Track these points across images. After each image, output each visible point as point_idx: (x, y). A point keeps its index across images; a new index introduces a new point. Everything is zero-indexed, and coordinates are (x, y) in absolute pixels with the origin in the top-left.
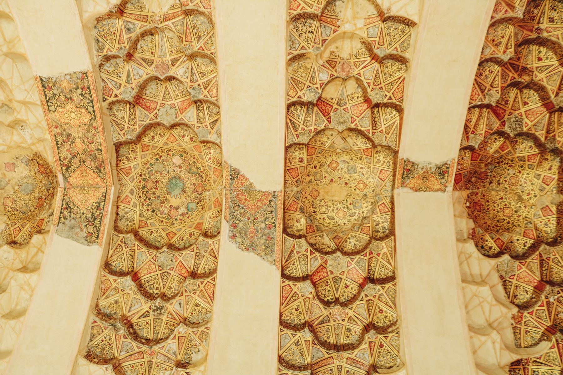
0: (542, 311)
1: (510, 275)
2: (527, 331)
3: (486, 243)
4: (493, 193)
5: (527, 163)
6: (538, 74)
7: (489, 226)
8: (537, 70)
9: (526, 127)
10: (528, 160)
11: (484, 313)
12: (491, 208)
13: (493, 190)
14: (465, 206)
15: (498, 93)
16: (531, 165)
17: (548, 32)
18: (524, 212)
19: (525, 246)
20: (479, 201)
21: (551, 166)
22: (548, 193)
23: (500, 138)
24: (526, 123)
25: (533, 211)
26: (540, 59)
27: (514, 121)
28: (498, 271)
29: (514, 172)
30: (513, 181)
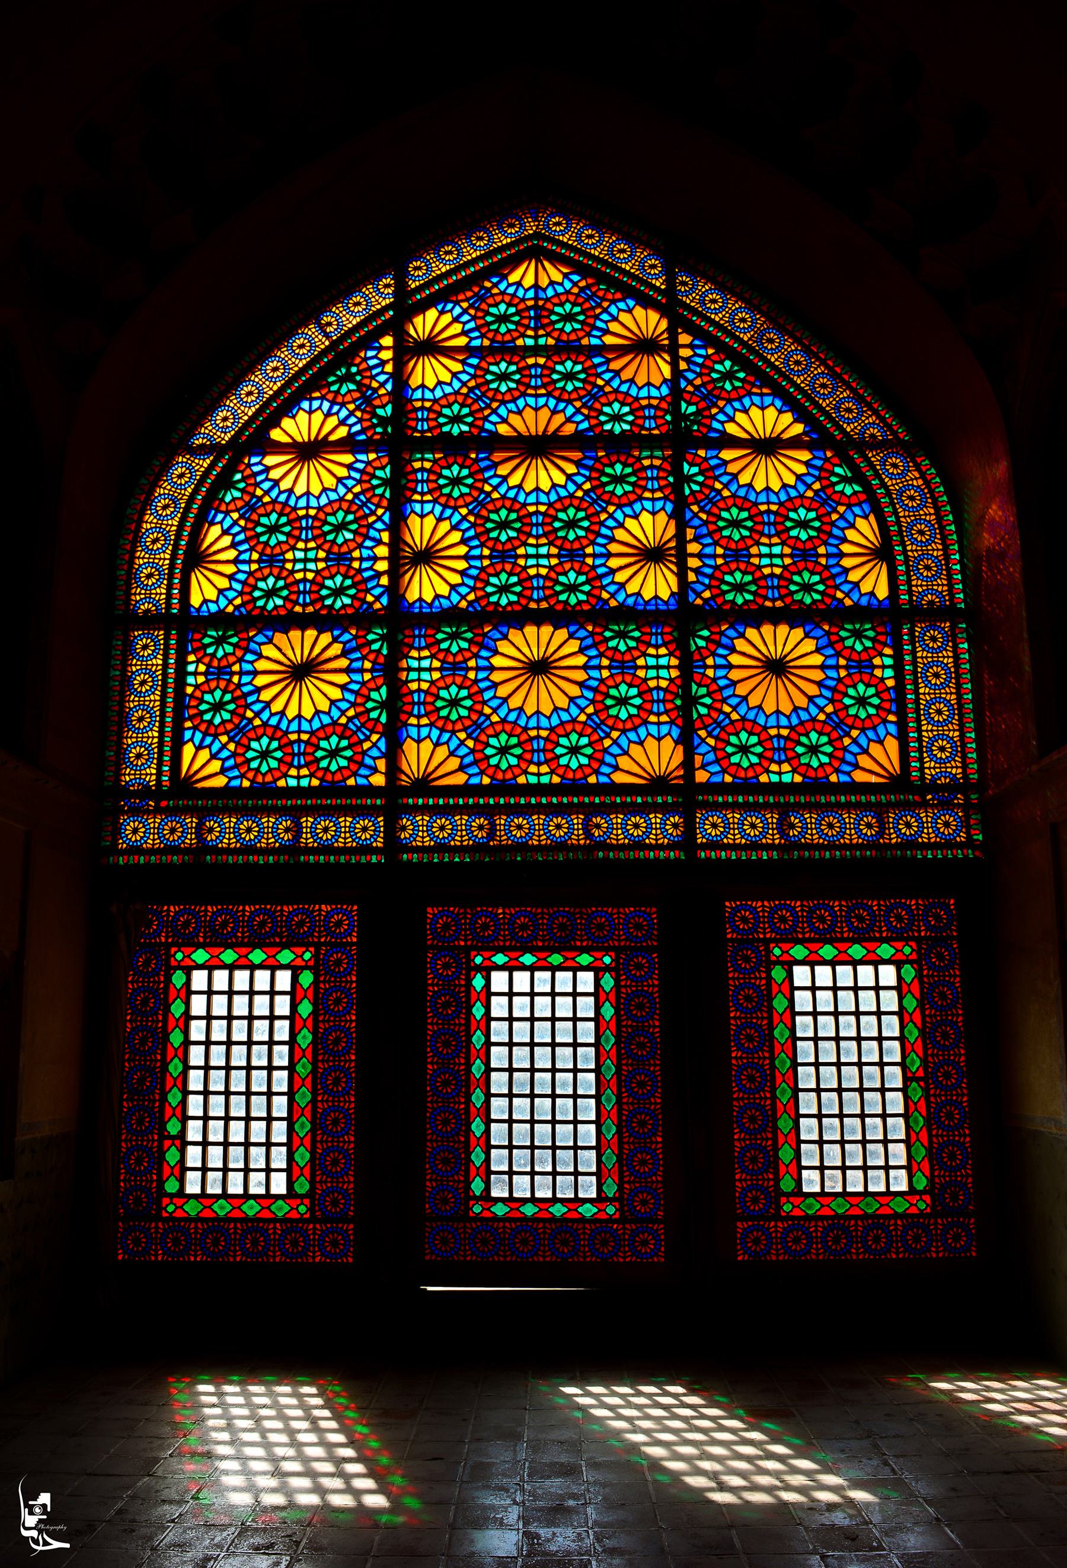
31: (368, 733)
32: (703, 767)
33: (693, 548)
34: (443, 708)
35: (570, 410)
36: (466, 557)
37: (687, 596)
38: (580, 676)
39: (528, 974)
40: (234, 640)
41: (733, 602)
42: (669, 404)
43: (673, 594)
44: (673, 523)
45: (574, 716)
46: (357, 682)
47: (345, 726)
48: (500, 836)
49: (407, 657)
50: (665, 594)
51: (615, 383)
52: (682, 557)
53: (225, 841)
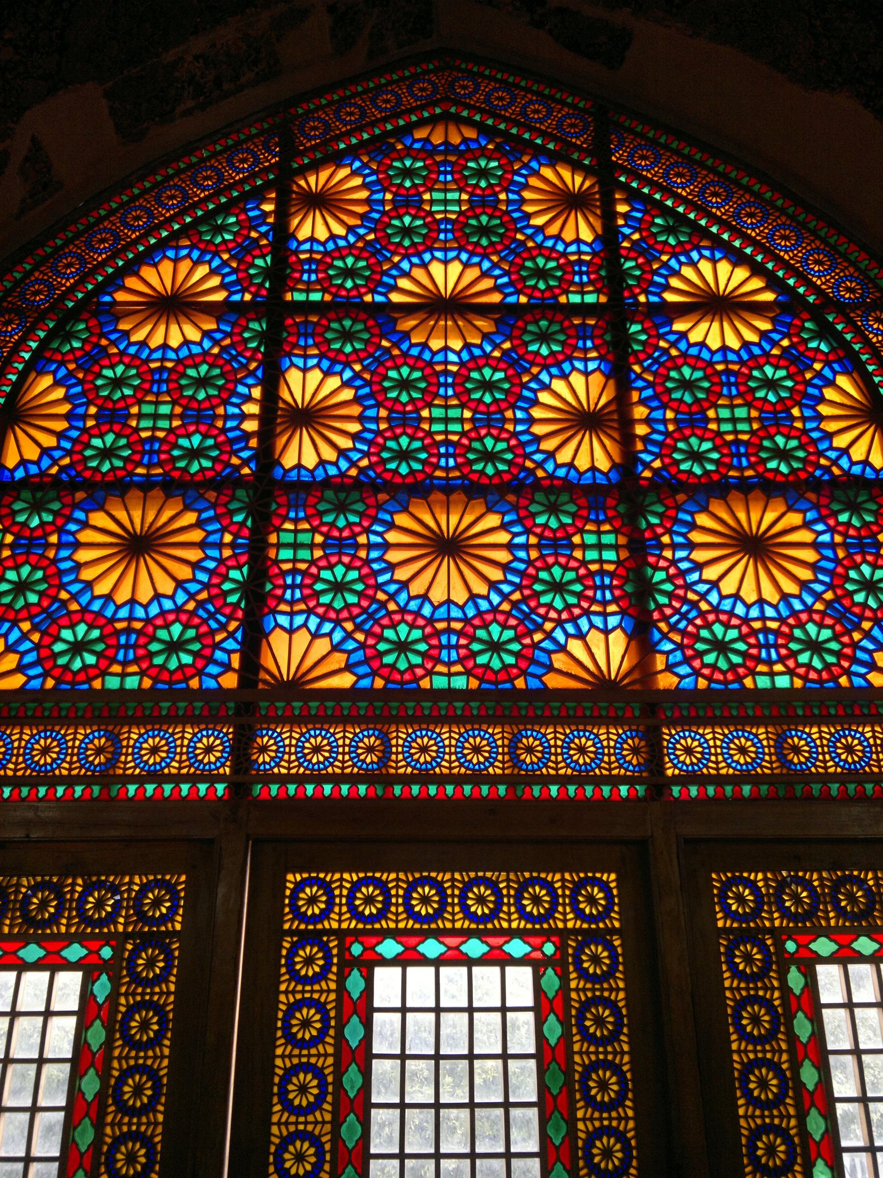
31: (223, 619)
32: (670, 668)
33: (640, 412)
34: (324, 592)
35: (486, 265)
36: (361, 419)
37: (636, 467)
38: (502, 556)
39: (432, 970)
40: (56, 506)
41: (690, 472)
42: (602, 259)
44: (611, 383)
46: (213, 559)
47: (193, 613)
48: (397, 762)
49: (279, 530)
50: (603, 464)
52: (627, 423)
53: (11, 766)
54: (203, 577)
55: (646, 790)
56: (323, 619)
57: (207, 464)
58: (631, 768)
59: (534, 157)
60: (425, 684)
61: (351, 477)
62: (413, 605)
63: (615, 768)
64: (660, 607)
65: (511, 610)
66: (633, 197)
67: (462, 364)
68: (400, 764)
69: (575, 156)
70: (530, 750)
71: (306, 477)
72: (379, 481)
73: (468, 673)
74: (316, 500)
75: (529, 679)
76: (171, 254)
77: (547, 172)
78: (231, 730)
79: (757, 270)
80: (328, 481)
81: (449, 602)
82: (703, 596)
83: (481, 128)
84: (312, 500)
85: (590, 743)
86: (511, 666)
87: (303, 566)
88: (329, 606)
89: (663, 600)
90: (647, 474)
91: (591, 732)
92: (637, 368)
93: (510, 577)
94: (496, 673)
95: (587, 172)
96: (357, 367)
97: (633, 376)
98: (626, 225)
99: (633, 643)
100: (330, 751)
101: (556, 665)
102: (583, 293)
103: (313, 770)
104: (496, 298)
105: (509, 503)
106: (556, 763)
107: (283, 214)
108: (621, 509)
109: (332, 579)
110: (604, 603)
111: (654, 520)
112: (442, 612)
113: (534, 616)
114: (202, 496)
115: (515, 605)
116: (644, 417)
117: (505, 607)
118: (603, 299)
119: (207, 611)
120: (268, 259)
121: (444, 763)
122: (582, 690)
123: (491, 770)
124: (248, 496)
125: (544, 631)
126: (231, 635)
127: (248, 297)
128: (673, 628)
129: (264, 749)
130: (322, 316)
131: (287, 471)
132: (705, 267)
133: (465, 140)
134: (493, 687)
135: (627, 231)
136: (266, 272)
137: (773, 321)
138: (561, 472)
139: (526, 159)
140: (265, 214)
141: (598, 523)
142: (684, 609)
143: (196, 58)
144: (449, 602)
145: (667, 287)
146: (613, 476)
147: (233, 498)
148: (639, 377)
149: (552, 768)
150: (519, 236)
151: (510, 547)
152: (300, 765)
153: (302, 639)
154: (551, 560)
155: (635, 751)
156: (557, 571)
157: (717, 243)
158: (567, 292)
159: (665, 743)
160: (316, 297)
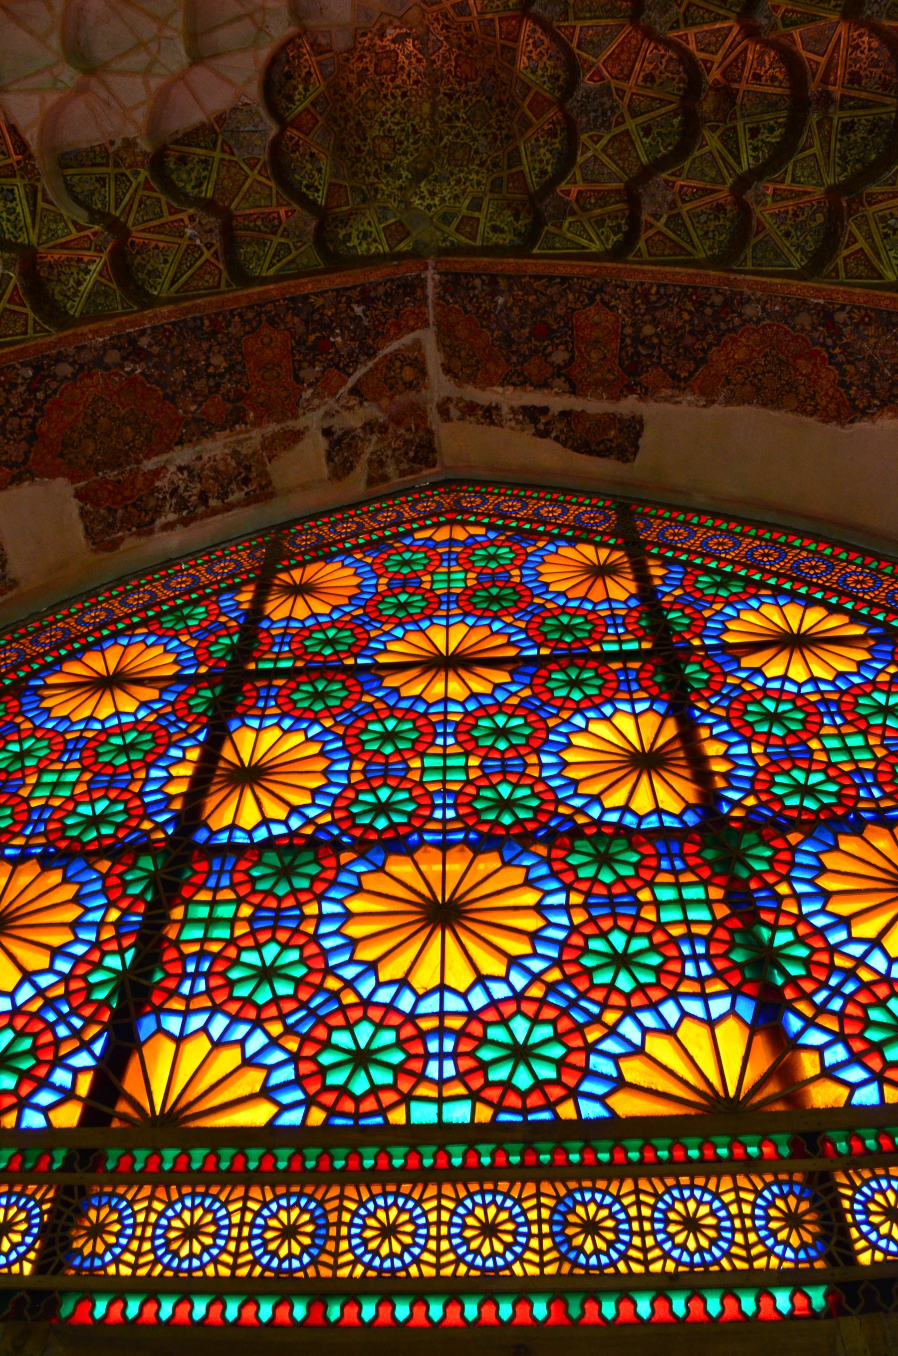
0: (157, 210)
1: (232, 142)
2: (104, 180)
3: (301, 87)
4: (426, 107)
5: (505, 174)
6: (718, 133)
7: (344, 97)
8: (727, 129)
9: (591, 137)
10: (512, 175)
11: (122, 56)
12: (388, 105)
13: (434, 106)
14: (385, 20)
15: (672, 28)
16: (501, 185)
17: (820, 124)
18: (387, 186)
19: (307, 186)
20: (402, 68)
21: (502, 231)
22: (438, 233)
23: (560, 88)
24: (600, 138)
25: (393, 204)
26: (754, 133)
27: (603, 104)
28: (234, 109)
29: (481, 149)
30: (459, 155)
33: (713, 749)
38: (531, 923)
41: (801, 808)
43: (688, 807)
45: (519, 987)
49: (188, 902)
51: (561, 601)
54: (63, 966)
55: (826, 1296)
56: (235, 1019)
57: (107, 830)
58: (789, 1254)
59: (550, 542)
60: (397, 1117)
61: (306, 836)
62: (384, 996)
63: (759, 1256)
64: (792, 981)
65: (545, 995)
66: (666, 563)
67: (467, 713)
68: (343, 1259)
69: (598, 538)
70: (591, 1227)
71: (240, 838)
72: (345, 839)
73: (474, 1097)
74: (248, 865)
75: (582, 1103)
76: (125, 642)
77: (567, 551)
78: (50, 1195)
79: (833, 610)
80: (270, 842)
81: (442, 988)
82: (861, 961)
83: (490, 527)
84: (243, 865)
85: (704, 1210)
86: (548, 1082)
87: (215, 948)
88: (247, 1001)
89: (795, 970)
90: (737, 813)
91: (705, 1190)
92: (701, 705)
93: (541, 950)
94: (524, 1095)
95: (613, 548)
96: (328, 723)
97: (697, 713)
98: (665, 584)
99: (759, 1040)
100: (215, 1235)
101: (629, 1077)
102: (620, 642)
103: (179, 1269)
104: (511, 652)
105: (538, 855)
106: (644, 1250)
107: (259, 601)
108: (709, 854)
109: (259, 964)
110: (701, 980)
111: (759, 866)
112: (430, 1005)
113: (583, 1003)
114: (90, 867)
115: (551, 988)
116: (721, 753)
117: (536, 992)
118: (646, 645)
119: (58, 1012)
120: (235, 638)
121: (426, 1257)
122: (677, 1117)
123: (517, 1269)
124: (155, 865)
125: (605, 1025)
126: (86, 1046)
127: (203, 670)
128: (821, 1009)
129: (98, 1231)
130: (290, 680)
131: (213, 834)
132: (770, 611)
133: (471, 536)
134: (520, 1119)
135: (666, 589)
136: (231, 648)
137: (869, 650)
138: (613, 817)
139: (541, 544)
140: (240, 603)
141: (673, 871)
142: (834, 981)
143: (181, 469)
144: (442, 988)
145: (726, 630)
146: (690, 819)
147: (133, 866)
148: (705, 713)
149: (637, 1261)
150: (537, 600)
151: (539, 909)
152: (158, 1260)
153: (197, 1049)
154: (606, 924)
155: (793, 1220)
156: (618, 939)
157: (777, 592)
158: (600, 642)
159: (846, 1204)
160: (287, 664)
